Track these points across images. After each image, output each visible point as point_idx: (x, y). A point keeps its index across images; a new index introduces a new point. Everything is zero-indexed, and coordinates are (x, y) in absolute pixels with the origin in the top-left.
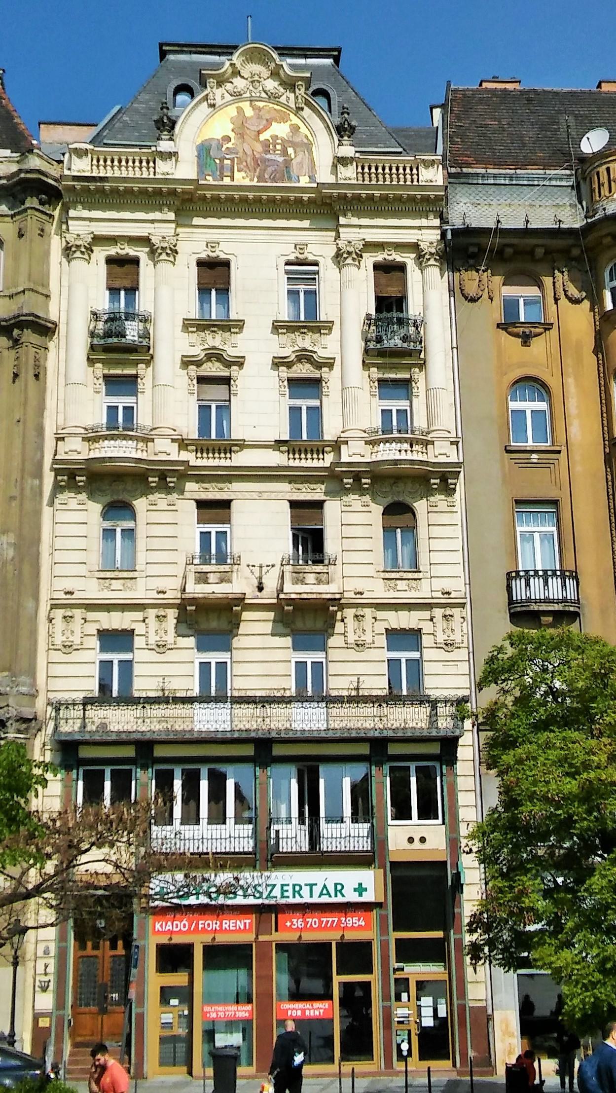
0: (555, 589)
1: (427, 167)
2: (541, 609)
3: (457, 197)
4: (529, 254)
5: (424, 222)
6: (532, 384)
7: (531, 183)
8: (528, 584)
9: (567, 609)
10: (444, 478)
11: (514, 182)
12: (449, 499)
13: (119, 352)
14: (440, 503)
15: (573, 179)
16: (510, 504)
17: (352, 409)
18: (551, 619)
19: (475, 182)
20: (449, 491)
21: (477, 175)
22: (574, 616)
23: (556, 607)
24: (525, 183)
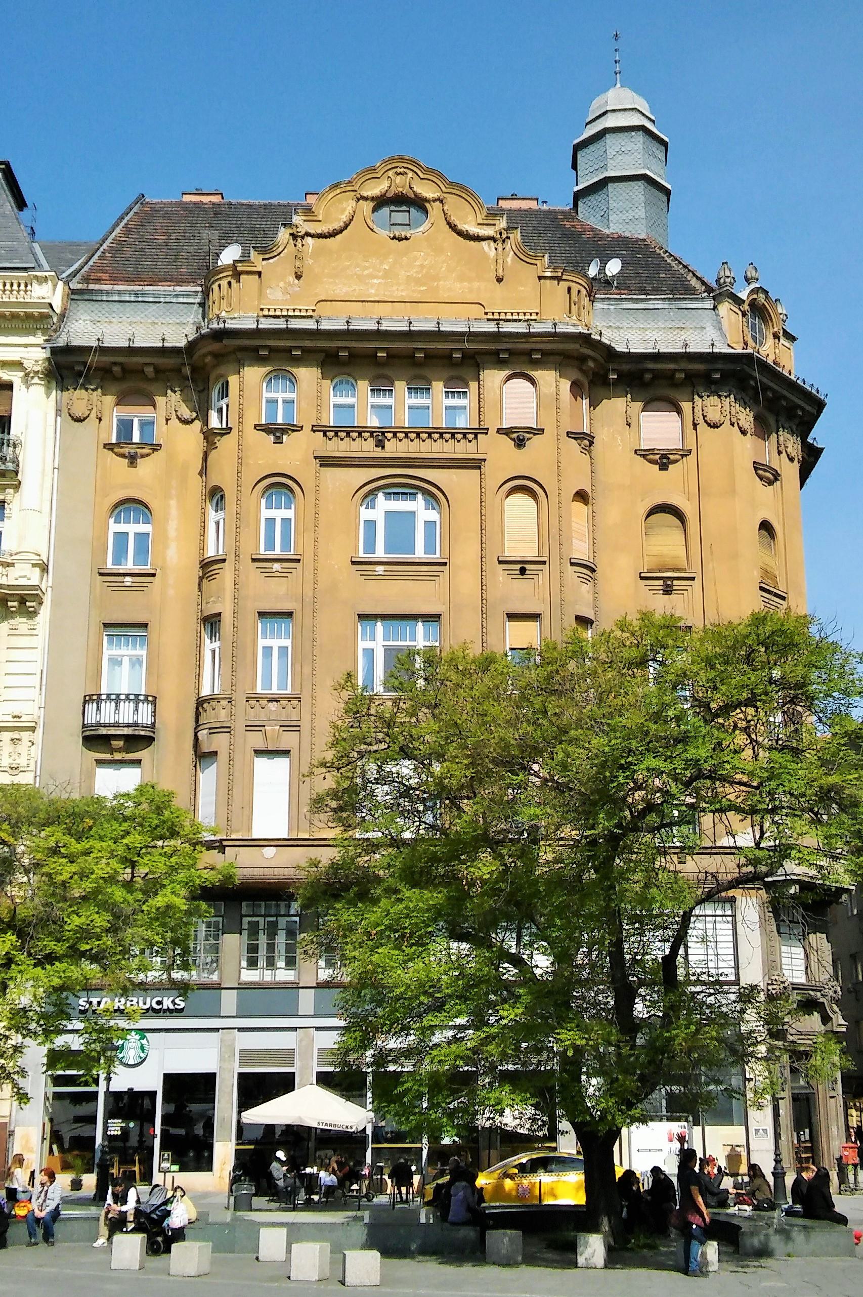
0: (126, 713)
1: (40, 283)
2: (109, 733)
3: (79, 314)
4: (137, 372)
5: (31, 340)
6: (131, 506)
7: (157, 300)
8: (98, 709)
9: (137, 733)
10: (23, 600)
11: (140, 299)
12: (30, 622)
14: (21, 627)
15: (200, 295)
16: (96, 626)
18: (121, 743)
19: (99, 298)
20: (32, 614)
21: (101, 292)
22: (148, 741)
23: (126, 731)
24: (151, 299)
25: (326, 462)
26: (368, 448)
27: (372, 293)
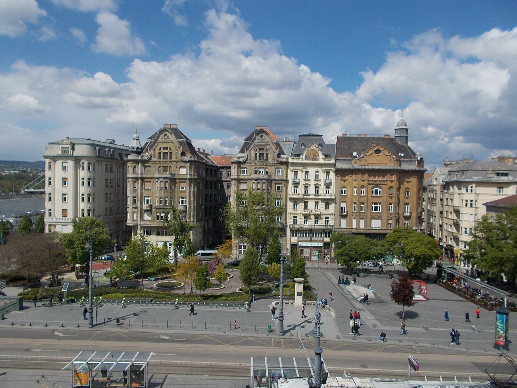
13: (296, 185)
17: (322, 190)
25: (368, 184)
26: (373, 182)
27: (374, 162)
